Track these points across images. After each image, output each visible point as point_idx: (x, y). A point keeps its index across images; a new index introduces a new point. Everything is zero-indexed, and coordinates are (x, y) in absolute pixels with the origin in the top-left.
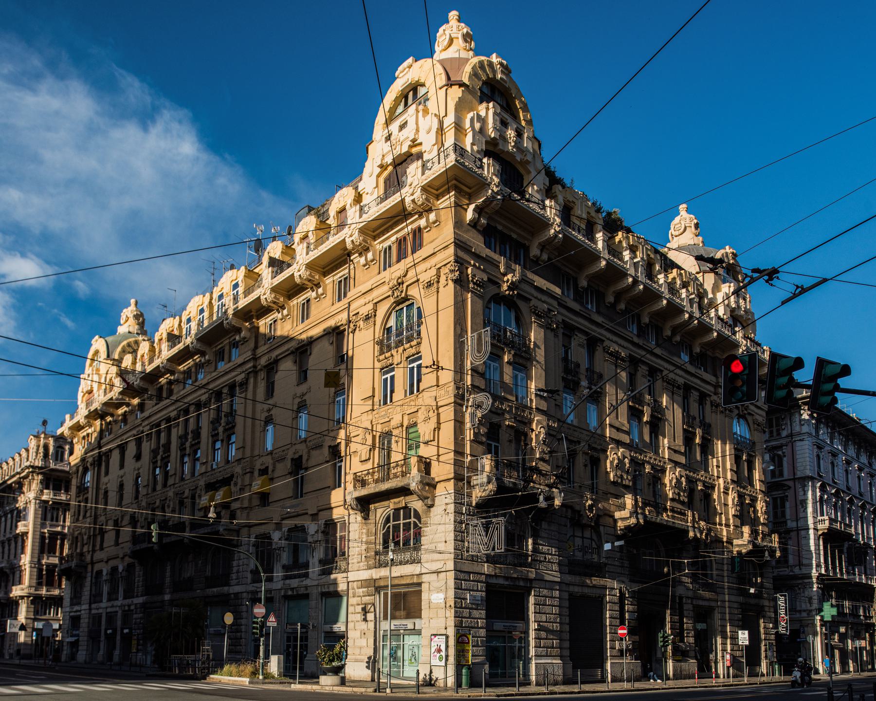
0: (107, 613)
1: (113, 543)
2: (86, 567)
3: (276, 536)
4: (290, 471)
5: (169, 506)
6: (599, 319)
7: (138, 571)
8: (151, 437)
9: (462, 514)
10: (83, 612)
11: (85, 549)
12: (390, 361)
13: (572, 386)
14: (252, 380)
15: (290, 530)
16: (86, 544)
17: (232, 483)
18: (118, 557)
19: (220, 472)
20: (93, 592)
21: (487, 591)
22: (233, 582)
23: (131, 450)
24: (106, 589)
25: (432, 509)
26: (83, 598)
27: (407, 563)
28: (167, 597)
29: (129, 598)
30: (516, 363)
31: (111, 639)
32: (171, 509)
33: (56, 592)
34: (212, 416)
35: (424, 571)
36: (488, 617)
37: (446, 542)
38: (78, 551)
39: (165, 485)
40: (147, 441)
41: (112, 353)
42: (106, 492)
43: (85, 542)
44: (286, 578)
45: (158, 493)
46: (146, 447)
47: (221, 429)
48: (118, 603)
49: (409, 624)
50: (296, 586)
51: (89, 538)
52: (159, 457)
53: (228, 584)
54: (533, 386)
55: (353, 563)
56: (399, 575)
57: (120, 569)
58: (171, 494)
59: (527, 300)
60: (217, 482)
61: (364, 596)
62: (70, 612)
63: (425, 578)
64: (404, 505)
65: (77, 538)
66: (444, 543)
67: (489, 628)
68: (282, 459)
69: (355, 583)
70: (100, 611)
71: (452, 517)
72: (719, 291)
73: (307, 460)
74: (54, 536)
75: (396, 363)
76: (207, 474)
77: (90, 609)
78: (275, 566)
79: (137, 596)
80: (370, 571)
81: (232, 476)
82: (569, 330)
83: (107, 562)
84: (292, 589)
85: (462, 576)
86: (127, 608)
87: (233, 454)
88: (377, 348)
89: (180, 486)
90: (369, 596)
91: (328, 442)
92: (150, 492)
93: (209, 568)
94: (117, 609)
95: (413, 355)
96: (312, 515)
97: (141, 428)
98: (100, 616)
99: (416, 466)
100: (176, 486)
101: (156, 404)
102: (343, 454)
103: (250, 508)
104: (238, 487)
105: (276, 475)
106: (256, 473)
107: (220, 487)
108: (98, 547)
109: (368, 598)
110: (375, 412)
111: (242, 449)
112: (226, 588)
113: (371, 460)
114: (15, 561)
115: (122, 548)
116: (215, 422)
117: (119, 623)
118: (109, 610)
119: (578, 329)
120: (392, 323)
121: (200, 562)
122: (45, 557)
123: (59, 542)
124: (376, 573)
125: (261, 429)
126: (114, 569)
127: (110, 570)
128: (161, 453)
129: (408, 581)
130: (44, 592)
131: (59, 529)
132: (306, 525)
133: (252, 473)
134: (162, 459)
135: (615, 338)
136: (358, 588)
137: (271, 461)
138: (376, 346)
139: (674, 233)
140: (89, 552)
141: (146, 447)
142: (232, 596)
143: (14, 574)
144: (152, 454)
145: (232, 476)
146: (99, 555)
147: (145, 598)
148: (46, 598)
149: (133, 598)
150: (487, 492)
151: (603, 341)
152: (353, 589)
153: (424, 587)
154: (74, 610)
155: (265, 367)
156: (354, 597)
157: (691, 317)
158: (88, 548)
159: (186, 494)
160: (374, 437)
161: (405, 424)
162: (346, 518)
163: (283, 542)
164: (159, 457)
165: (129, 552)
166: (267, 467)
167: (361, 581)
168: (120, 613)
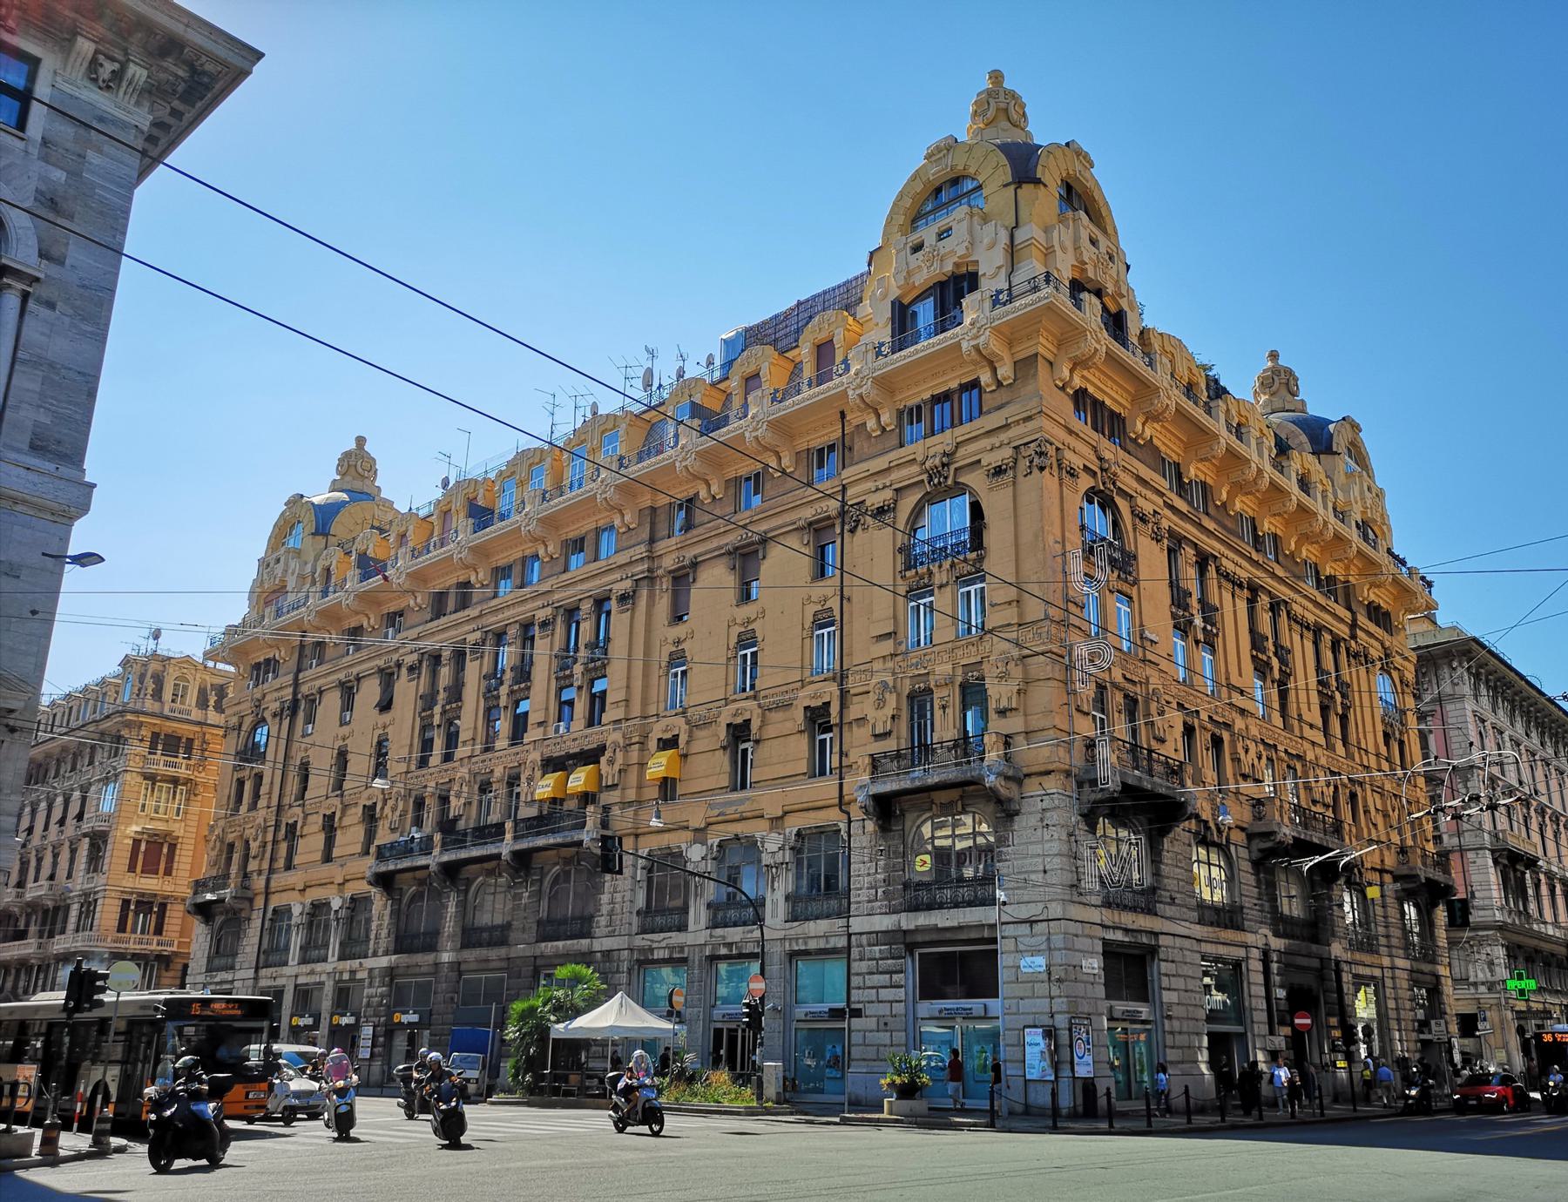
0: (296, 986)
1: (318, 856)
2: (251, 900)
3: (695, 853)
4: (725, 743)
5: (458, 796)
7: (380, 906)
8: (420, 674)
12: (926, 581)
14: (644, 593)
16: (254, 858)
17: (603, 760)
19: (574, 740)
20: (265, 945)
21: (1105, 954)
23: (370, 692)
26: (240, 958)
27: (970, 904)
28: (446, 957)
30: (1118, 591)
32: (462, 801)
34: (556, 648)
35: (1005, 918)
36: (1108, 997)
37: (1045, 872)
39: (448, 758)
43: (253, 852)
44: (714, 925)
45: (431, 770)
46: (407, 691)
47: (578, 669)
48: (328, 967)
49: (976, 1004)
50: (737, 939)
51: (264, 845)
52: (437, 709)
53: (587, 934)
56: (955, 924)
57: (336, 903)
58: (463, 772)
61: (882, 959)
65: (231, 846)
66: (1042, 875)
68: (707, 724)
70: (280, 982)
76: (546, 742)
77: (256, 979)
78: (692, 903)
79: (375, 954)
80: (895, 917)
81: (602, 749)
83: (303, 891)
84: (729, 945)
88: (900, 559)
89: (484, 761)
90: (893, 958)
92: (413, 767)
93: (544, 904)
94: (324, 978)
100: (474, 760)
101: (432, 620)
102: (834, 719)
103: (639, 803)
104: (617, 767)
106: (652, 744)
107: (576, 766)
108: (281, 863)
109: (890, 962)
110: (899, 658)
112: (585, 942)
113: (894, 735)
117: (326, 1005)
118: (301, 980)
123: (165, 850)
124: (909, 921)
129: (974, 935)
132: (758, 835)
133: (643, 743)
134: (444, 712)
135: (1231, 555)
136: (869, 945)
137: (685, 727)
138: (899, 556)
140: (260, 872)
141: (407, 691)
144: (419, 702)
145: (602, 749)
146: (281, 879)
149: (366, 957)
152: (860, 945)
153: (1001, 946)
154: (217, 979)
155: (670, 572)
156: (861, 960)
158: (260, 865)
162: (843, 826)
165: (368, 874)
166: (676, 737)
167: (877, 933)
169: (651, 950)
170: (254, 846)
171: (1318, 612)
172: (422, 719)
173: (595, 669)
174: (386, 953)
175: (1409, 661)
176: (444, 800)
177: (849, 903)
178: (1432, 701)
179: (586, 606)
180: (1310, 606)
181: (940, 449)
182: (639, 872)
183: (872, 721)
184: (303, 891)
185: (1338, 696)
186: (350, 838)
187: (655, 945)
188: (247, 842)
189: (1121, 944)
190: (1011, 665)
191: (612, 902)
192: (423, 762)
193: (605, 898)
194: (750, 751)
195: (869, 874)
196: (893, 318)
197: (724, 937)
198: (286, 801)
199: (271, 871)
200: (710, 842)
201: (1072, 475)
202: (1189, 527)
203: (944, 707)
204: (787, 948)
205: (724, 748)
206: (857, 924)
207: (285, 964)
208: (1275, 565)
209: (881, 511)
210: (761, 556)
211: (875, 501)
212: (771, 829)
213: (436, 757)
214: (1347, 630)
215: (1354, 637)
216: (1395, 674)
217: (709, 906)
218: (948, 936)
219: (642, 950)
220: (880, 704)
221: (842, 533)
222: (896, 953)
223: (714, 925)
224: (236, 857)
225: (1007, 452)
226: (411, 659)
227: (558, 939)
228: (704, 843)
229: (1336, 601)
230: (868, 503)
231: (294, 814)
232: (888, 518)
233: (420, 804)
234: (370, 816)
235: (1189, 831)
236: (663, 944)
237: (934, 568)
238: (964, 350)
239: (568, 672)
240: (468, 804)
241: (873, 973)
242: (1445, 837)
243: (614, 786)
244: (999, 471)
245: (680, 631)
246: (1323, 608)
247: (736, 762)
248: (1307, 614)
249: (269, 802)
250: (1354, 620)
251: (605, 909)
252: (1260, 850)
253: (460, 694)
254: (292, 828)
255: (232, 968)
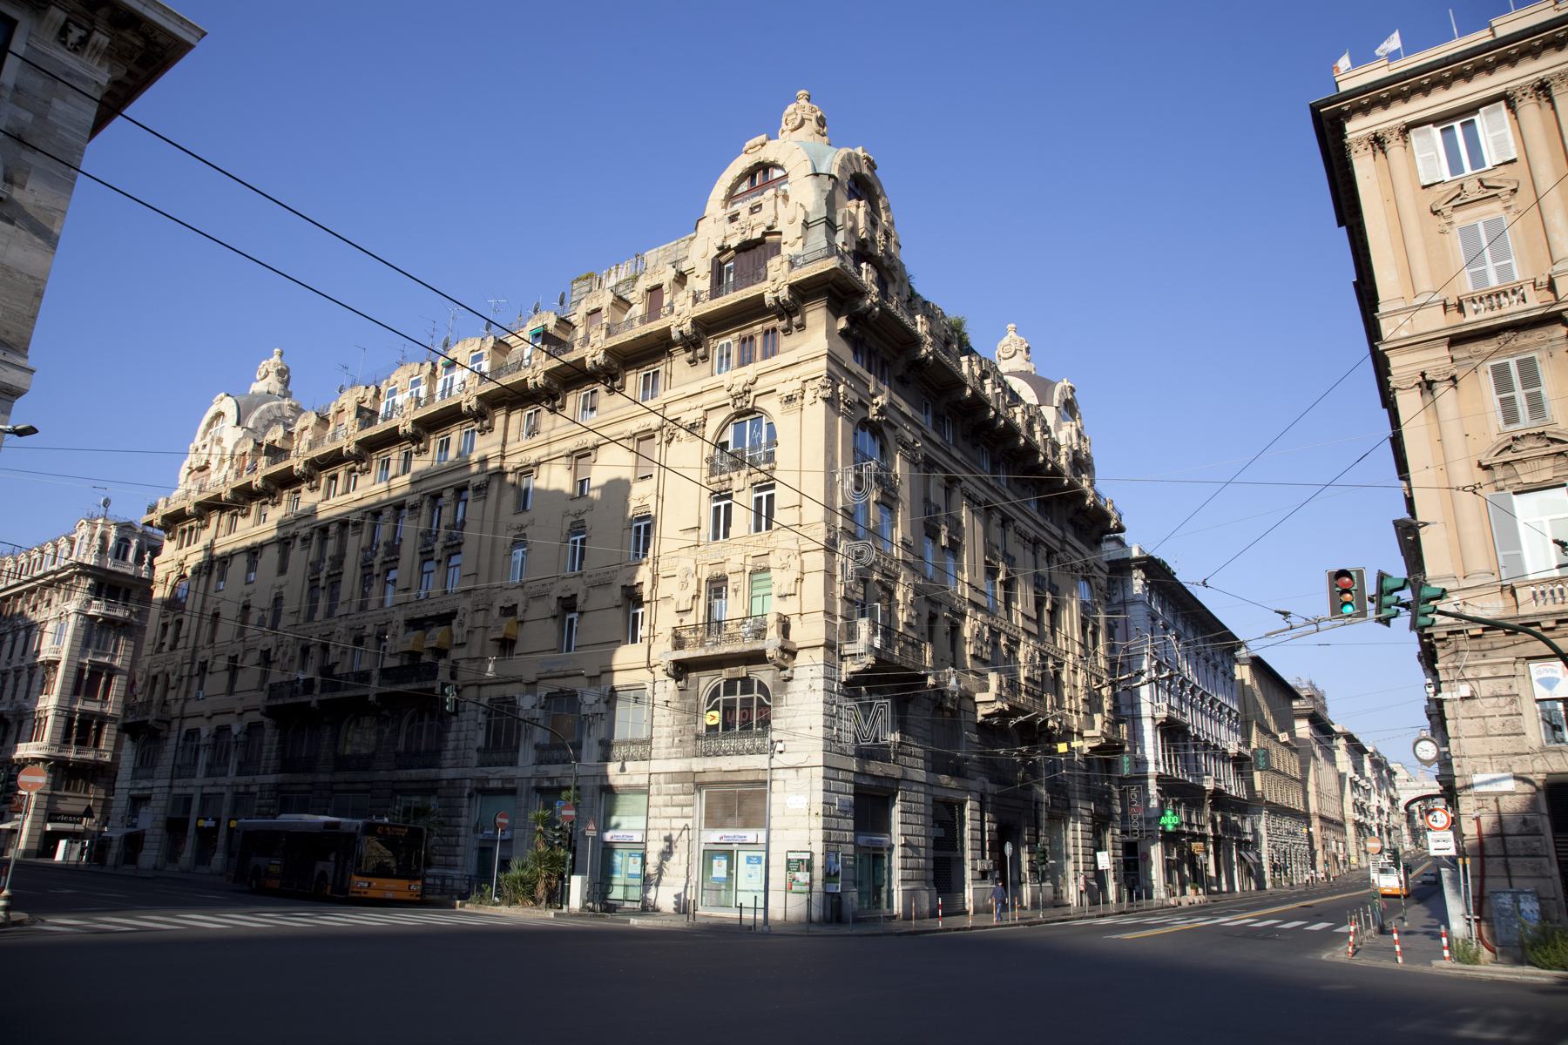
0: (202, 794)
1: (223, 690)
2: (169, 723)
3: (526, 702)
4: (556, 613)
6: (958, 455)
7: (270, 737)
9: (833, 692)
10: (155, 790)
11: (171, 695)
13: (933, 534)
15: (549, 696)
16: (173, 688)
17: (455, 622)
18: (233, 712)
19: (433, 604)
20: (179, 761)
22: (446, 763)
24: (203, 758)
25: (789, 683)
27: (749, 752)
29: (248, 774)
31: (207, 837)
33: (90, 756)
38: (157, 696)
39: (329, 614)
40: (302, 549)
41: (245, 418)
42: (216, 615)
44: (540, 762)
47: (438, 546)
48: (227, 781)
51: (180, 679)
54: (898, 534)
55: (659, 748)
57: (236, 729)
58: (341, 627)
59: (893, 427)
60: (427, 618)
62: (130, 789)
63: (778, 774)
64: (744, 675)
65: (155, 678)
67: (855, 843)
69: (662, 776)
70: (190, 791)
71: (820, 696)
72: (1061, 429)
73: (585, 601)
74: (97, 670)
75: (735, 489)
76: (409, 606)
78: (522, 743)
79: (265, 773)
80: (688, 761)
81: (453, 614)
82: (929, 465)
83: (209, 718)
84: (551, 779)
85: (832, 773)
86: (242, 789)
87: (456, 581)
90: (684, 794)
91: (621, 581)
92: (301, 621)
93: (402, 740)
94: (224, 790)
95: (761, 482)
96: (590, 677)
97: (292, 530)
98: (188, 800)
99: (775, 627)
100: (350, 617)
104: (466, 629)
105: (529, 616)
107: (432, 626)
109: (682, 797)
111: (473, 577)
113: (694, 612)
114: (26, 704)
115: (242, 699)
116: (428, 536)
117: (225, 811)
118: (207, 790)
119: (937, 463)
120: (729, 436)
121: (387, 730)
122: (80, 701)
123: (103, 679)
124: (697, 764)
125: (506, 552)
126: (223, 730)
127: (214, 731)
128: (326, 569)
129: (751, 777)
130: (72, 754)
131: (106, 660)
136: (666, 783)
139: (1001, 353)
140: (177, 700)
142: (445, 782)
143: (21, 723)
144: (309, 567)
145: (453, 614)
147: (280, 775)
148: (74, 763)
149: (258, 774)
150: (864, 666)
151: (961, 481)
154: (140, 786)
156: (658, 795)
157: (1046, 460)
159: (369, 630)
160: (699, 581)
161: (748, 569)
162: (649, 686)
163: (538, 713)
164: (323, 575)
166: (515, 606)
168: (228, 796)
169: (488, 780)
170: (173, 679)
171: (1037, 529)
172: (311, 581)
173: (453, 546)
174: (274, 772)
175: (1104, 572)
176: (325, 648)
177: (651, 749)
178: (1119, 603)
179: (448, 494)
180: (1032, 524)
181: (743, 380)
182: (480, 716)
183: (676, 600)
184: (209, 718)
185: (1048, 595)
186: (249, 677)
187: (491, 776)
188: (167, 675)
189: (869, 787)
190: (792, 557)
191: (458, 740)
192: (310, 618)
193: (451, 736)
194: (575, 620)
195: (667, 726)
196: (712, 272)
197: (546, 772)
198: (199, 644)
199: (186, 699)
200: (538, 694)
201: (849, 407)
202: (941, 455)
203: (736, 591)
204: (598, 783)
205: (554, 617)
206: (656, 766)
207: (194, 776)
208: (1006, 490)
209: (692, 428)
210: (592, 458)
211: (688, 418)
212: (590, 686)
213: (319, 615)
214: (1058, 544)
215: (1063, 550)
216: (1092, 581)
217: (537, 747)
218: (730, 777)
219: (479, 780)
220: (684, 585)
221: (660, 443)
222: (686, 790)
223: (540, 762)
224: (158, 688)
225: (797, 384)
226: (304, 532)
227: (412, 768)
228: (534, 694)
229: (1051, 522)
230: (683, 420)
231: (205, 654)
232: (699, 432)
233: (305, 651)
234: (266, 658)
235: (929, 699)
236: (497, 776)
237: (734, 475)
238: (766, 301)
239: (430, 548)
240: (344, 653)
241: (667, 806)
242: (1123, 708)
243: (462, 645)
244: (790, 399)
245: (522, 519)
246: (1041, 527)
247: (564, 630)
248: (1029, 531)
249: (187, 643)
250: (1064, 537)
251: (451, 745)
252: (983, 715)
253: (341, 563)
254: (203, 666)
255: (152, 777)
